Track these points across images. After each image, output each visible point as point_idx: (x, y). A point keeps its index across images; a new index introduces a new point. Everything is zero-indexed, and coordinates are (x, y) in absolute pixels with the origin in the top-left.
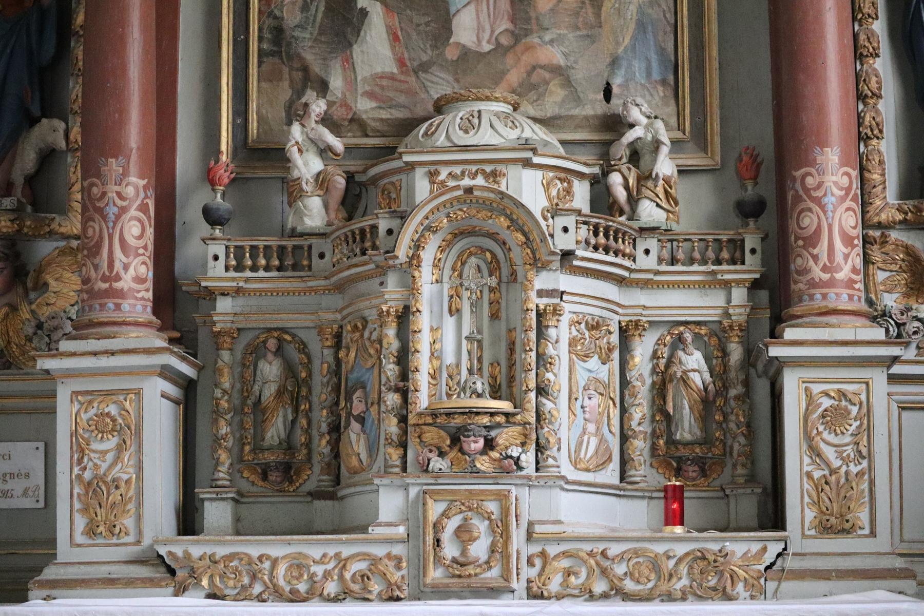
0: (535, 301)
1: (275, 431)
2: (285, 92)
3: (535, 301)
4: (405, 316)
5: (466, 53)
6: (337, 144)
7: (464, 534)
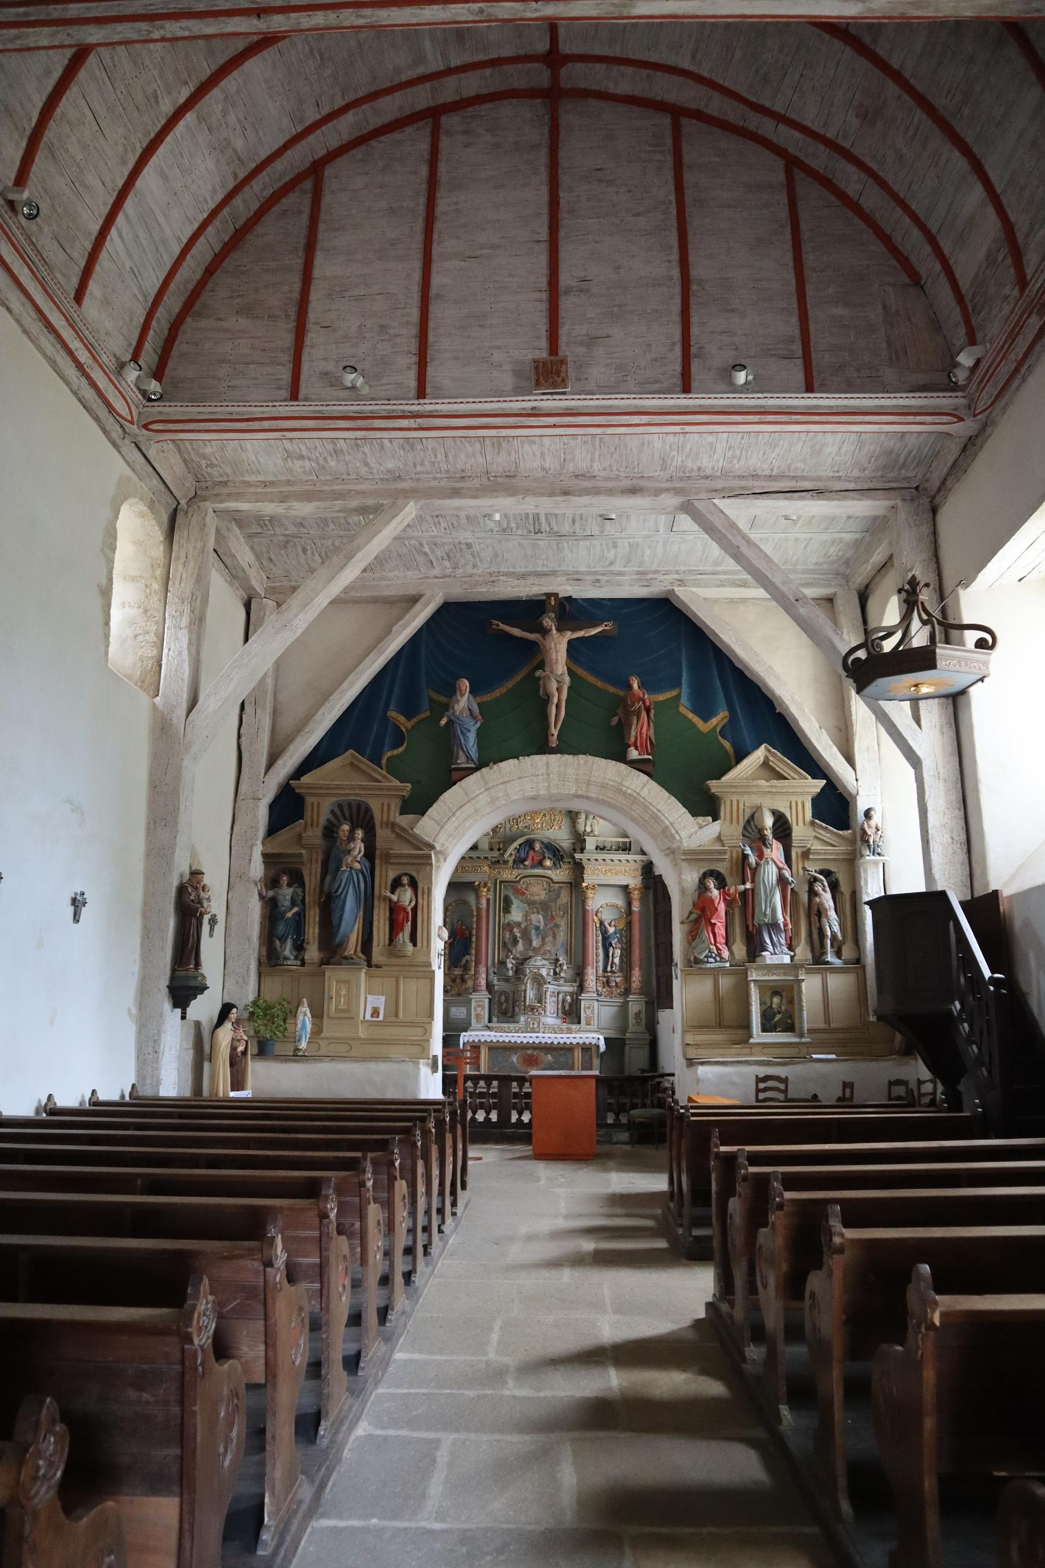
1: (504, 1007)
2: (505, 952)
4: (525, 991)
5: (535, 948)
7: (533, 1024)
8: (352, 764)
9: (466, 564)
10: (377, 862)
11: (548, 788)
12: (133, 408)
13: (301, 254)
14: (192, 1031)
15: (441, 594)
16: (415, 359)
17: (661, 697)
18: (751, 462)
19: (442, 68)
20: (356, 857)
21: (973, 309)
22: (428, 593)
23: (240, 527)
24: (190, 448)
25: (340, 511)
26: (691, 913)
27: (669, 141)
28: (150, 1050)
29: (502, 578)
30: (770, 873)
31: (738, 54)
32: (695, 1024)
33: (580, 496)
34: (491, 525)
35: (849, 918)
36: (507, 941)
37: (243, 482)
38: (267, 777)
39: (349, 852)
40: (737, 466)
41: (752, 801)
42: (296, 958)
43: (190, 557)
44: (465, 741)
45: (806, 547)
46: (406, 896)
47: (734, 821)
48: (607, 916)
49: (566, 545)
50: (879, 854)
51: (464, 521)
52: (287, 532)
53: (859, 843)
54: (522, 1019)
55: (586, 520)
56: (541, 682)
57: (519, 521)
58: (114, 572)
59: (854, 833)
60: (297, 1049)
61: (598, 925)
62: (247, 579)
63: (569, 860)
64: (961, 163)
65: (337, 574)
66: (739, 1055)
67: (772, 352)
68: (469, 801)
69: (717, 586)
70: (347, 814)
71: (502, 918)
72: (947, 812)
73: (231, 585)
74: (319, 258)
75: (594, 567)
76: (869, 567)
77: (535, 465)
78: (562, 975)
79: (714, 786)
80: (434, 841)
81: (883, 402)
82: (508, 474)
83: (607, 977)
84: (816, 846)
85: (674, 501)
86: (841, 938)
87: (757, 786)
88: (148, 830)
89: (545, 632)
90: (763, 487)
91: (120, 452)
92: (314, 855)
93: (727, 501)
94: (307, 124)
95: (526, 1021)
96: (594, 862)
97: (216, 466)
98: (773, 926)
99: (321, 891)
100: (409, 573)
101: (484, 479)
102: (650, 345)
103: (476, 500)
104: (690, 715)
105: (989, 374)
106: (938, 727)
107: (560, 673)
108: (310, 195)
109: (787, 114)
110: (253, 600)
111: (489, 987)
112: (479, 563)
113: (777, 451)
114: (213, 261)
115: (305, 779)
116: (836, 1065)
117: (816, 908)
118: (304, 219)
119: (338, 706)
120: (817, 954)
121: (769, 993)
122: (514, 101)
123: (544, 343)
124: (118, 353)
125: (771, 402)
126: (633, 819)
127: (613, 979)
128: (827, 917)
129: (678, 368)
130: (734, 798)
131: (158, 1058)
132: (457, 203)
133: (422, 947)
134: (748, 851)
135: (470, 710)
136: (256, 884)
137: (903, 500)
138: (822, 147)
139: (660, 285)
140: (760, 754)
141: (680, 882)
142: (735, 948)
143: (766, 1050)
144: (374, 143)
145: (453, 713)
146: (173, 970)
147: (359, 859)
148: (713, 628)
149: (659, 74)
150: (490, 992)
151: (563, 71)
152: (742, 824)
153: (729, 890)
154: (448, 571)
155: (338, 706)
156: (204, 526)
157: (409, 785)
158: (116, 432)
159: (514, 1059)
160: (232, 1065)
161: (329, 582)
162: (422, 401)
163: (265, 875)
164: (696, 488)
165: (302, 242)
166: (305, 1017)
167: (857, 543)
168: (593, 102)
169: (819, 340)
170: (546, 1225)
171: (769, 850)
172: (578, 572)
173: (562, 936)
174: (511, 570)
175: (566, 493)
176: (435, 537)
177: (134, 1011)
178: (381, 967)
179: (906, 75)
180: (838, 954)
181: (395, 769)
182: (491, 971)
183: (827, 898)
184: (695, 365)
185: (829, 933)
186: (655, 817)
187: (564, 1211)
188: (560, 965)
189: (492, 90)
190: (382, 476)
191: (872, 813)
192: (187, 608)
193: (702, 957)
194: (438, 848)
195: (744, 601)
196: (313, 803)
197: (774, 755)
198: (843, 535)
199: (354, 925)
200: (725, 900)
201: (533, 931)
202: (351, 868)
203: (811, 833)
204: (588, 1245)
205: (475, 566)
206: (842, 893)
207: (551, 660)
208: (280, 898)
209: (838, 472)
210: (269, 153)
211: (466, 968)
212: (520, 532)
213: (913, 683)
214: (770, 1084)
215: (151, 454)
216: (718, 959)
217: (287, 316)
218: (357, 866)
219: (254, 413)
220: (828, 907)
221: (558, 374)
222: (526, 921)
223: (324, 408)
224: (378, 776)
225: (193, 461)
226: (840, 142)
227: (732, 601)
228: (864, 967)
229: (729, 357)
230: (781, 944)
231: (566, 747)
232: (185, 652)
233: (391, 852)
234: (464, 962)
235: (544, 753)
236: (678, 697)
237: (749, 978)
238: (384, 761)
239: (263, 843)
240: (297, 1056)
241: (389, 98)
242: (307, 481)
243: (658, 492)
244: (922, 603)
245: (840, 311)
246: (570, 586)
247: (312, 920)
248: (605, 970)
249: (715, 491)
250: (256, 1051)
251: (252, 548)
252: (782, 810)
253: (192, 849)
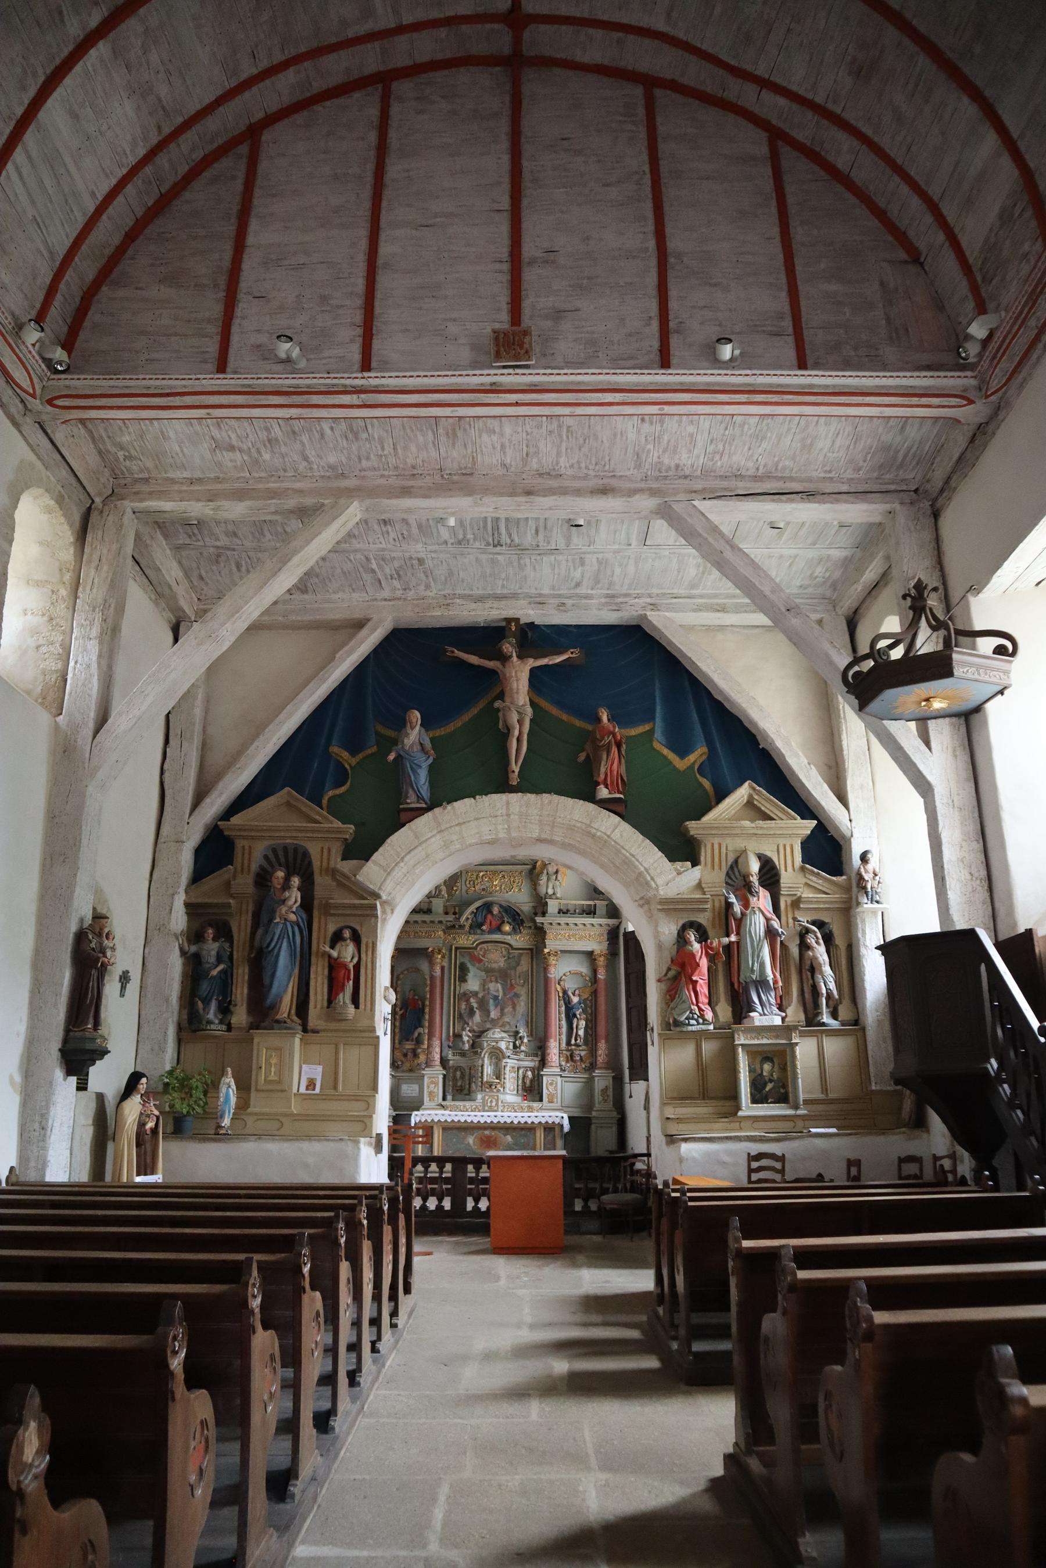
0: (504, 1064)
1: (459, 1083)
2: (461, 1024)
3: (504, 1064)
4: (482, 1066)
5: (493, 1019)
6: (470, 1035)
7: (491, 1102)
8: (288, 804)
9: (418, 585)
10: (316, 913)
11: (509, 830)
12: (36, 380)
13: (234, 220)
14: (93, 1105)
15: (390, 618)
16: (359, 331)
17: (633, 732)
18: (735, 458)
19: (393, 25)
20: (291, 908)
21: (984, 278)
22: (375, 617)
23: (166, 536)
24: (104, 435)
25: (276, 513)
26: (669, 969)
27: (641, 111)
28: (36, 1126)
29: (458, 601)
30: (757, 925)
31: (718, 10)
32: (675, 1095)
33: (545, 496)
34: (445, 534)
35: (845, 974)
36: (463, 1012)
37: (167, 479)
38: (192, 817)
39: (284, 901)
40: (719, 464)
41: (733, 844)
42: (221, 1022)
43: (104, 559)
44: (415, 778)
45: (790, 565)
46: (347, 952)
47: (716, 867)
48: (570, 985)
49: (527, 561)
50: (877, 902)
51: (415, 531)
52: (218, 543)
53: (855, 889)
54: (479, 1096)
55: (551, 530)
56: (501, 714)
57: (476, 531)
58: (10, 567)
59: (849, 879)
60: (219, 1127)
61: (561, 995)
62: (174, 597)
63: (530, 924)
64: (968, 108)
65: (269, 579)
66: (727, 1130)
67: (760, 329)
68: (420, 844)
69: (694, 611)
70: (282, 860)
71: (458, 988)
72: (964, 844)
73: (157, 604)
74: (254, 225)
75: (559, 590)
76: (860, 588)
77: (495, 462)
78: (523, 1048)
79: (693, 827)
80: (380, 889)
81: (885, 382)
82: (464, 471)
83: (571, 1050)
84: (807, 894)
85: (646, 503)
86: (837, 997)
87: (742, 828)
88: (43, 865)
89: (504, 659)
90: (749, 488)
91: (20, 432)
92: (244, 907)
93: (708, 503)
94: (244, 76)
95: (483, 1099)
96: (556, 926)
97: (135, 458)
98: (762, 983)
99: (252, 947)
100: (355, 595)
101: (438, 478)
102: (623, 319)
103: (427, 500)
104: (666, 751)
105: (1004, 347)
106: (950, 750)
107: (521, 703)
108: (245, 160)
109: (771, 79)
110: (182, 624)
111: (444, 1062)
112: (432, 584)
113: (764, 445)
114: (132, 229)
115: (235, 820)
116: (837, 1140)
117: (808, 963)
118: (239, 185)
119: (274, 740)
120: (810, 1016)
121: (759, 1059)
122: (472, 69)
123: (505, 316)
124: (17, 313)
125: (761, 380)
126: (603, 866)
127: (577, 1052)
128: (821, 973)
129: (656, 344)
130: (716, 841)
131: (44, 1136)
132: (408, 171)
133: (365, 1009)
134: (733, 899)
135: (421, 744)
136: (177, 939)
137: (901, 503)
138: (809, 115)
139: (634, 257)
140: (743, 792)
141: (656, 935)
142: (718, 1009)
143: (756, 1125)
144: (317, 108)
145: (403, 747)
146: (67, 1031)
147: (294, 909)
148: (689, 655)
149: (631, 37)
150: (444, 1068)
151: (526, 34)
152: (724, 869)
153: (711, 943)
154: (399, 593)
155: (274, 740)
156: (121, 526)
157: (352, 826)
158: (16, 407)
159: (471, 1140)
160: (139, 1145)
161: (261, 588)
162: (366, 374)
163: (189, 927)
164: (674, 489)
165: (235, 208)
166: (229, 1090)
167: (846, 562)
168: (557, 71)
169: (813, 317)
170: (507, 1338)
171: (755, 899)
172: (540, 595)
173: (522, 1007)
174: (467, 592)
175: (528, 493)
176: (383, 550)
177: (18, 1079)
178: (318, 1032)
179: (908, 15)
180: (834, 1015)
181: (336, 810)
182: (445, 1044)
183: (820, 952)
184: (674, 341)
185: (824, 991)
186: (627, 862)
187: (528, 1319)
188: (521, 1038)
189: (449, 55)
190: (323, 474)
191: (869, 856)
192: (98, 616)
193: (683, 1018)
194: (384, 897)
195: (722, 628)
196: (243, 847)
197: (759, 793)
198: (832, 552)
199: (287, 986)
200: (707, 954)
201: (491, 1001)
202: (285, 919)
203: (801, 880)
204: (561, 1366)
205: (428, 587)
206: (837, 946)
207: (511, 689)
208: (204, 953)
209: (830, 472)
210: (199, 107)
211: (418, 1041)
212: (477, 544)
213: (924, 696)
214: (764, 1162)
215: (59, 437)
216: (701, 1021)
217: (216, 286)
218: (293, 917)
219: (175, 387)
220: (822, 962)
221: (521, 346)
222: (484, 990)
223: (255, 382)
224: (317, 817)
225: (108, 452)
226: (830, 106)
227: (709, 629)
228: (864, 1029)
229: (714, 332)
230: (770, 1004)
231: (529, 785)
232: (94, 666)
233: (331, 901)
234: (416, 1034)
235: (504, 792)
236: (651, 732)
237: (736, 1043)
238: (325, 801)
239: (186, 892)
240: (218, 1135)
241: (333, 56)
242: (238, 478)
243: (632, 493)
244: (931, 609)
245: (833, 287)
246: (533, 609)
247: (240, 980)
248: (568, 1043)
249: (695, 492)
250: (170, 1128)
251: (180, 563)
252: (769, 854)
253: (98, 892)
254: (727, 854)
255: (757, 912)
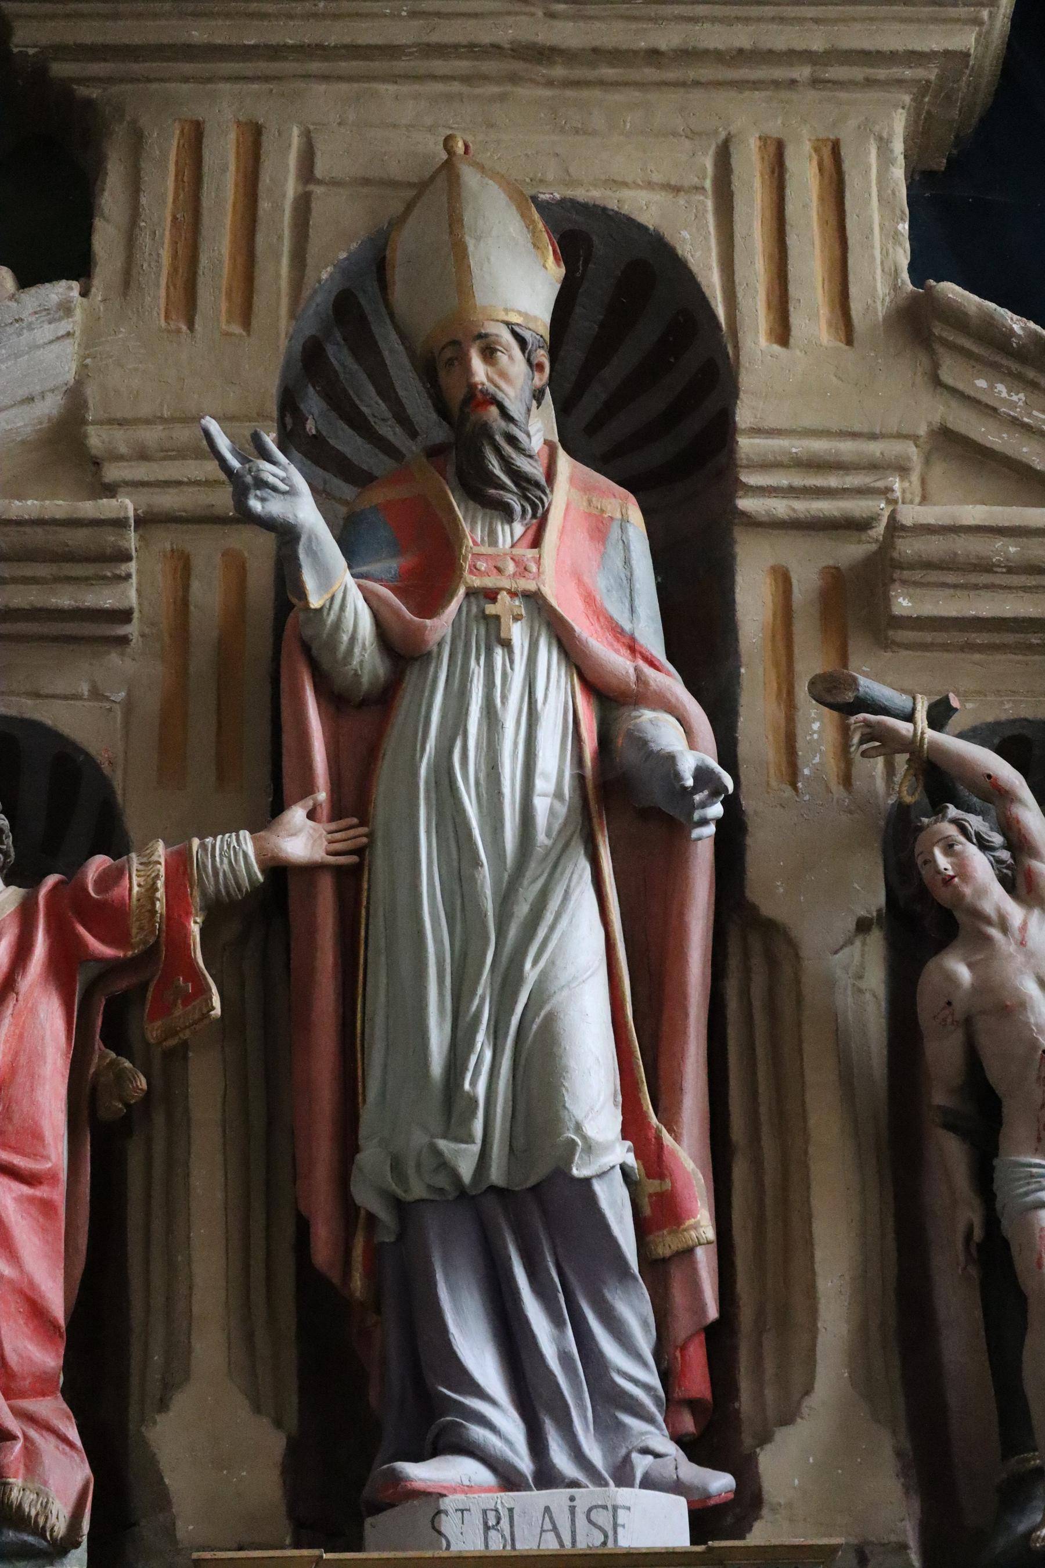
254: (303, 205)
255: (517, 633)
